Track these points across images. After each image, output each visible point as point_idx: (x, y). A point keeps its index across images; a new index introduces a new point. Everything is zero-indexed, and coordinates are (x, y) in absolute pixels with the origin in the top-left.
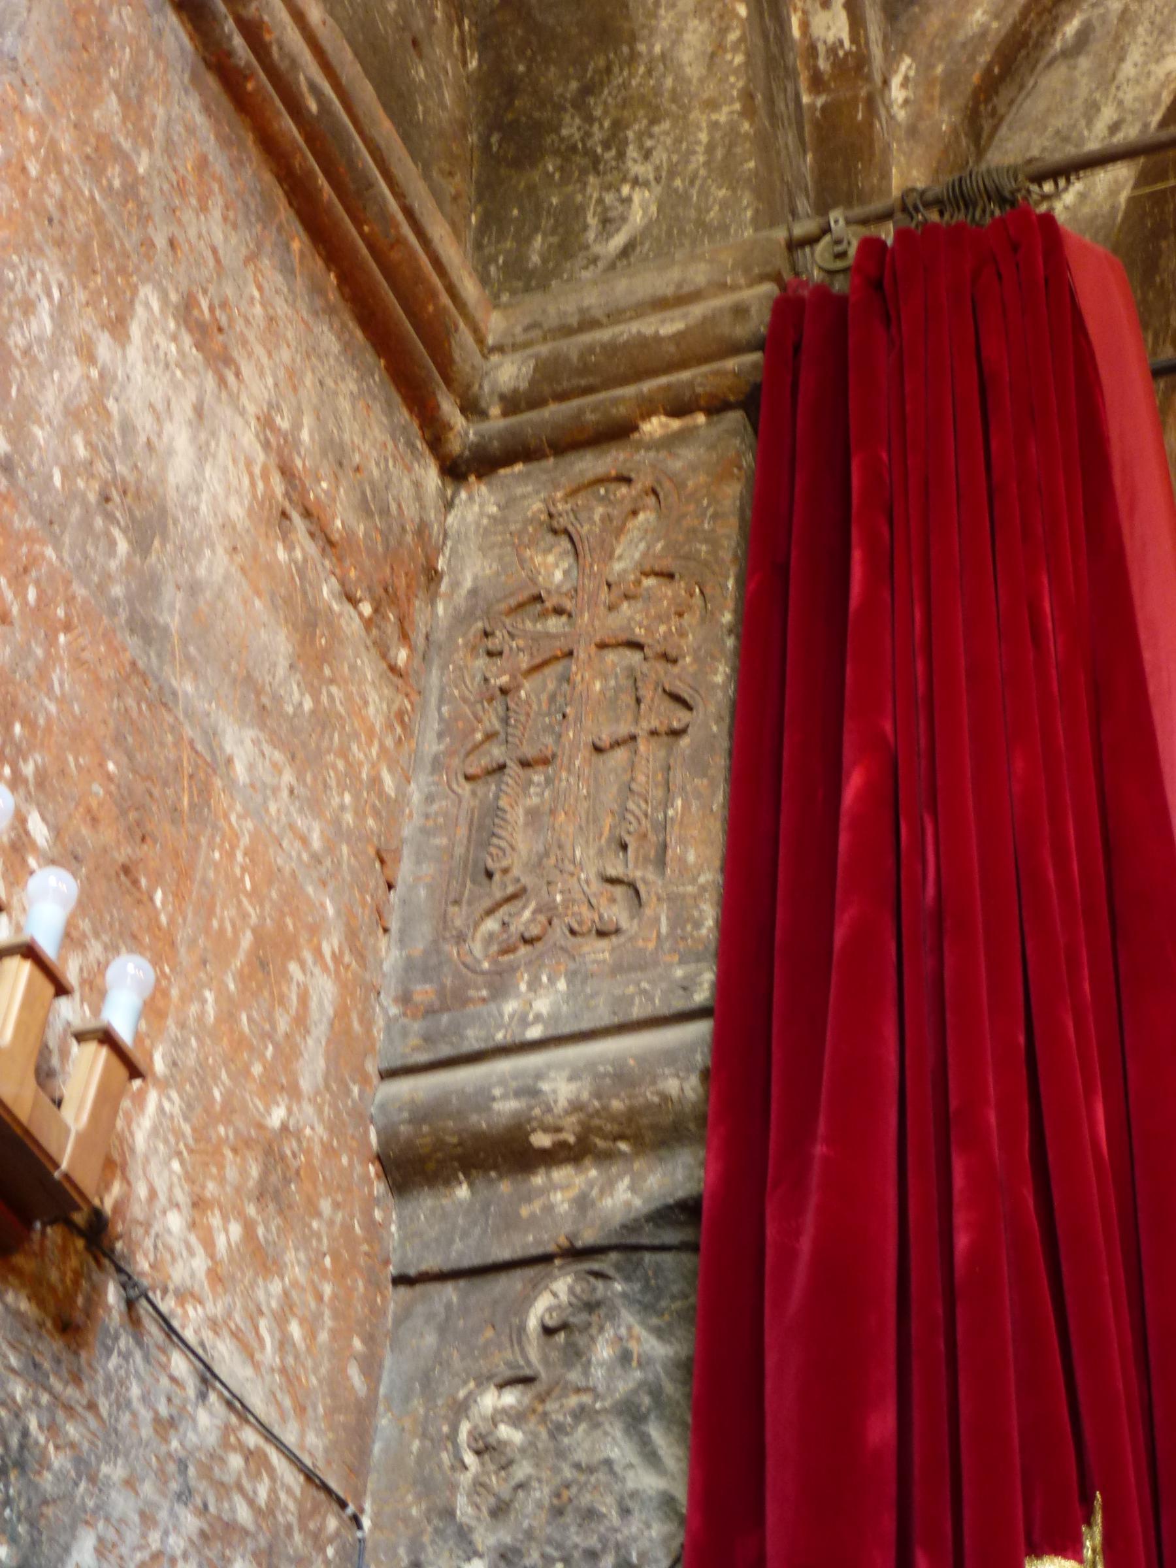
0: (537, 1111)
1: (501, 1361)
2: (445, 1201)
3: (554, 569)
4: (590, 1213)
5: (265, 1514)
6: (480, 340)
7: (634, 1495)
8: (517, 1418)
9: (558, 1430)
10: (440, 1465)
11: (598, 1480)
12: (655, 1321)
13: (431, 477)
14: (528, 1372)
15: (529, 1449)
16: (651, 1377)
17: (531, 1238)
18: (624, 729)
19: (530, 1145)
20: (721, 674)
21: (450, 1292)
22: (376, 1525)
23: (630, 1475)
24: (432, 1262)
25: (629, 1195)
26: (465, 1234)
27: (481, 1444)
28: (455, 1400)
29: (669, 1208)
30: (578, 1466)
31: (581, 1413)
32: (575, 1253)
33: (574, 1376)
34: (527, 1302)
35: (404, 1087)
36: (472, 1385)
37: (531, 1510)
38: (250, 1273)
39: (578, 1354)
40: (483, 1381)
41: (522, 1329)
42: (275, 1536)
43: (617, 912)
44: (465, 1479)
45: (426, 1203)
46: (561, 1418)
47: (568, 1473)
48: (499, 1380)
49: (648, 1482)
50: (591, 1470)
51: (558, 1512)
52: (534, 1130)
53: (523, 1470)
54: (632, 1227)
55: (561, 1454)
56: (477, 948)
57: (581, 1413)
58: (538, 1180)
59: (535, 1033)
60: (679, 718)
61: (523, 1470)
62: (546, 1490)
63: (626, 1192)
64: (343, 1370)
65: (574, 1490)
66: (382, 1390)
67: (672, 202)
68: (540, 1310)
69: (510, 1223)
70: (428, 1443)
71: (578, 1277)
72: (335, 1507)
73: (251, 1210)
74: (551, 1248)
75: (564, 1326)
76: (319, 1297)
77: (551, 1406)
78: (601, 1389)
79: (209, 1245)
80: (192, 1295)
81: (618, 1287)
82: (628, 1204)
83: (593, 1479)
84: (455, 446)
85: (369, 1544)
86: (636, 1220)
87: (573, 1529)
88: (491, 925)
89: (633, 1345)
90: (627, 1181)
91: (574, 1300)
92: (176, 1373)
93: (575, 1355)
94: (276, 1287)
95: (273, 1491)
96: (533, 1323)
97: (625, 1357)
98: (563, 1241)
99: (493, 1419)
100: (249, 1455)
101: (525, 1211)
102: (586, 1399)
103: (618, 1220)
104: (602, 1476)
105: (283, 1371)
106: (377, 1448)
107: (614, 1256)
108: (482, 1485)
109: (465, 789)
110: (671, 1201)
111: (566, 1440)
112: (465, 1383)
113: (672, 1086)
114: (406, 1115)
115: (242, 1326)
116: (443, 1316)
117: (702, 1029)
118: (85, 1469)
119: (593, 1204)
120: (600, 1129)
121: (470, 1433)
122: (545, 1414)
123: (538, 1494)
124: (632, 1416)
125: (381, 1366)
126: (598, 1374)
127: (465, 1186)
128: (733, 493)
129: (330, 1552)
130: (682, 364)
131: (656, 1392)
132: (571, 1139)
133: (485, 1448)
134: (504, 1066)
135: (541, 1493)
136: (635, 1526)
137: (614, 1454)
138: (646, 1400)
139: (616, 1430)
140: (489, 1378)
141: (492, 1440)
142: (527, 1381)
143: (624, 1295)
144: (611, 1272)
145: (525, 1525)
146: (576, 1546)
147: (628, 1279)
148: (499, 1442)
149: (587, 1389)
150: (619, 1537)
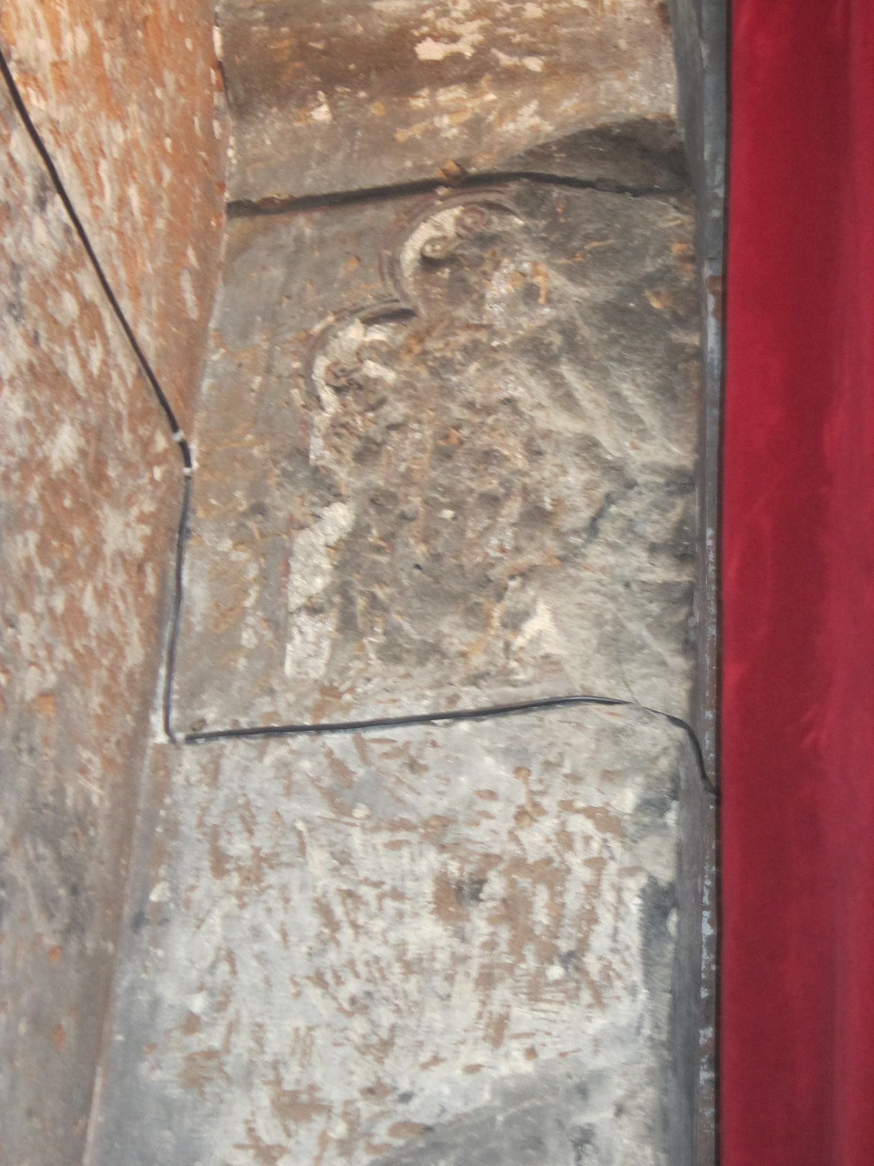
0: (429, 14)
1: (370, 292)
2: (297, 125)
4: (486, 139)
7: (546, 435)
8: (388, 355)
10: (289, 403)
11: (497, 420)
12: (563, 261)
14: (403, 305)
15: (406, 388)
16: (563, 316)
17: (409, 164)
19: (415, 55)
21: (304, 225)
22: (203, 466)
23: (538, 414)
24: (279, 191)
25: (536, 120)
26: (324, 159)
27: (343, 381)
28: (309, 336)
29: (590, 134)
30: (470, 405)
31: (472, 351)
32: (464, 182)
33: (463, 312)
34: (402, 233)
36: (331, 319)
37: (411, 450)
38: (93, 100)
39: (468, 290)
40: (344, 315)
41: (394, 263)
42: (105, 419)
44: (321, 419)
46: (449, 354)
47: (457, 412)
48: (363, 314)
50: (488, 410)
51: (445, 455)
52: (422, 38)
53: (397, 410)
54: (540, 152)
55: (448, 392)
58: (419, 103)
61: (397, 410)
62: (428, 432)
64: (177, 276)
65: (465, 432)
66: (212, 325)
68: (420, 239)
69: (383, 143)
70: (273, 379)
71: (469, 208)
72: (165, 423)
73: (99, 27)
74: (437, 174)
75: (451, 260)
76: (159, 177)
77: (434, 345)
78: (499, 325)
79: (57, 37)
80: (35, 79)
81: (519, 222)
82: (535, 129)
83: (490, 420)
85: (196, 486)
86: (545, 146)
87: (465, 473)
89: (539, 280)
90: (534, 105)
91: (463, 232)
92: (17, 157)
93: (463, 291)
94: (119, 135)
95: (105, 363)
96: (409, 255)
97: (530, 294)
98: (451, 166)
99: (358, 354)
100: (86, 306)
101: (402, 135)
102: (482, 336)
103: (523, 145)
104: (503, 416)
105: (121, 234)
106: (206, 384)
107: (514, 187)
108: (344, 426)
110: (591, 127)
111: (455, 379)
112: (322, 316)
114: (260, 14)
115: (83, 152)
116: (292, 249)
119: (490, 128)
120: (506, 38)
121: (328, 369)
122: (425, 352)
123: (418, 436)
125: (212, 298)
126: (495, 312)
127: (325, 109)
129: (158, 473)
131: (569, 332)
132: (468, 53)
133: (347, 384)
135: (422, 433)
136: (547, 469)
137: (519, 392)
138: (556, 340)
139: (522, 368)
140: (354, 312)
141: (356, 376)
142: (402, 315)
143: (526, 230)
144: (510, 205)
145: (403, 467)
146: (471, 491)
147: (530, 214)
148: (367, 378)
149: (480, 327)
150: (527, 480)
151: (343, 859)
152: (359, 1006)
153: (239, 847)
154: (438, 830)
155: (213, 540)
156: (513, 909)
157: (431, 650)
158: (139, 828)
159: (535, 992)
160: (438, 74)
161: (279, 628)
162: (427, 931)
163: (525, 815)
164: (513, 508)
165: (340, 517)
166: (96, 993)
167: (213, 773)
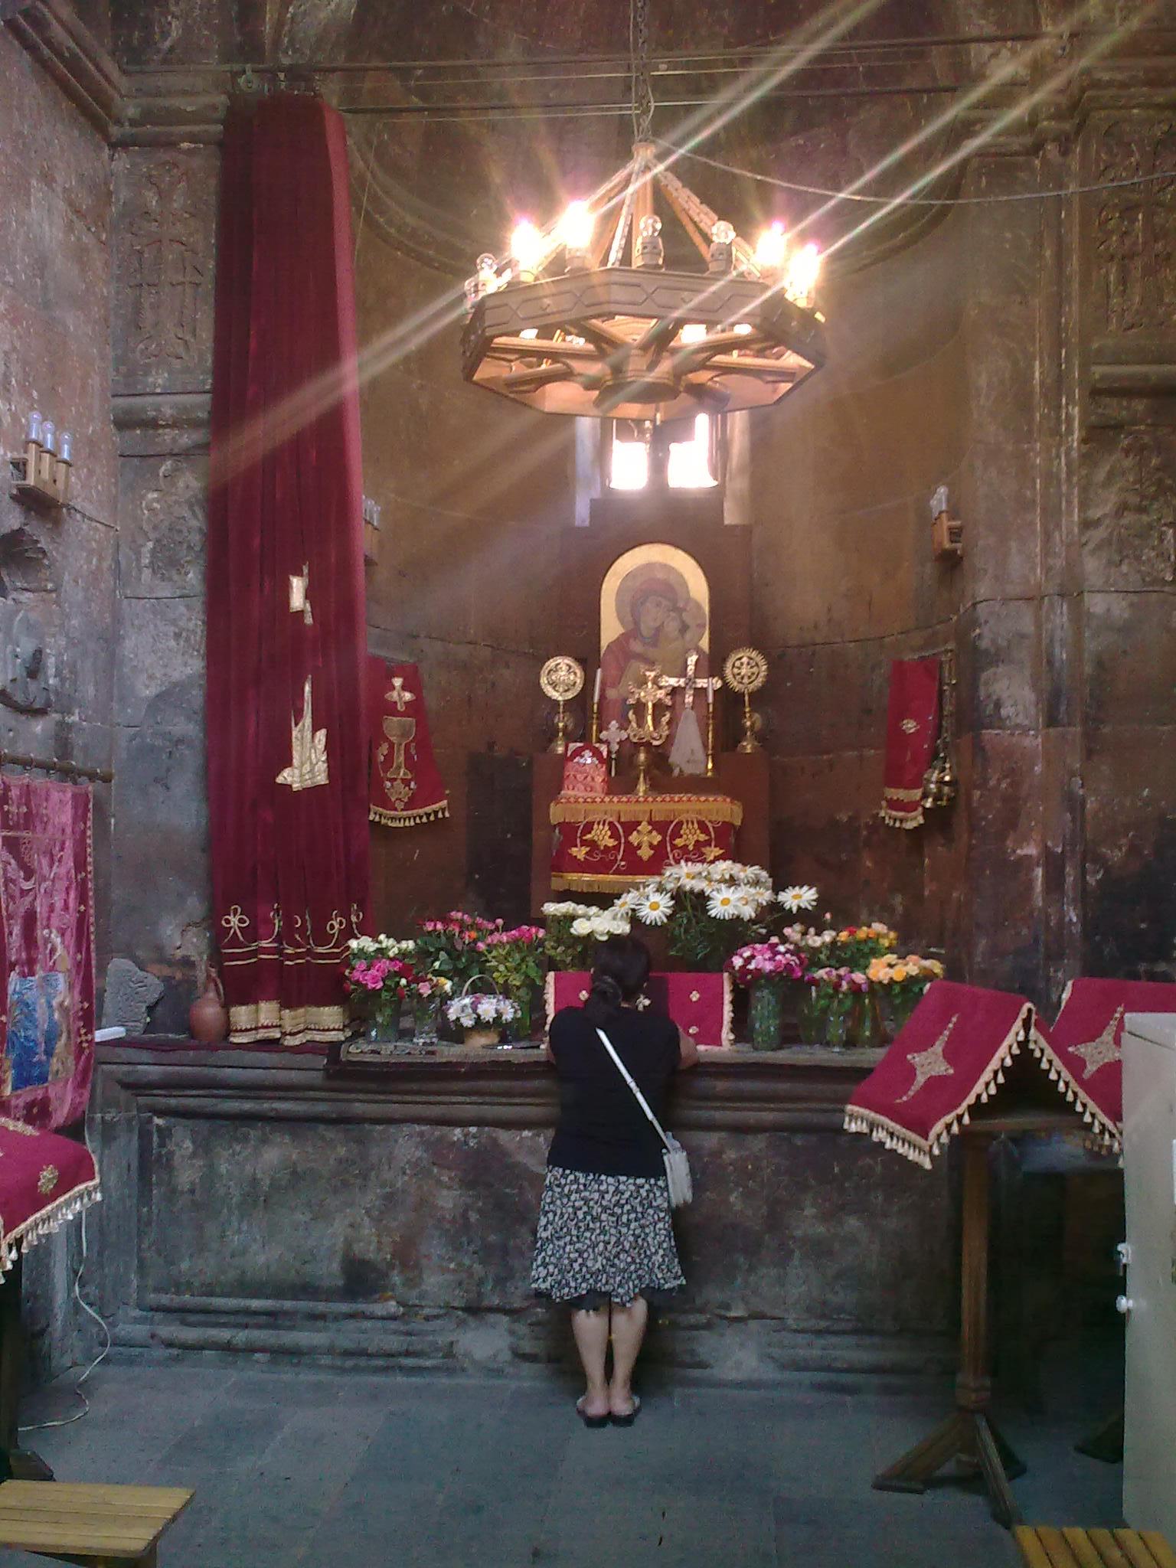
3: (152, 200)
5: (98, 542)
6: (119, 92)
8: (158, 501)
9: (170, 506)
13: (106, 152)
18: (181, 279)
20: (211, 265)
21: (136, 461)
35: (120, 401)
40: (149, 489)
43: (181, 351)
45: (127, 434)
49: (195, 523)
53: (161, 517)
54: (188, 449)
56: (138, 354)
57: (176, 502)
59: (158, 390)
60: (198, 279)
63: (186, 439)
67: (187, 29)
84: (113, 140)
88: (141, 346)
93: (174, 485)
109: (128, 290)
113: (200, 415)
117: (208, 396)
118: (64, 556)
124: (191, 506)
128: (213, 182)
130: (196, 122)
134: (150, 399)
135: (166, 523)
151: (156, 626)
152: (161, 658)
153: (136, 622)
154: (174, 622)
155: (125, 549)
156: (187, 640)
157: (170, 579)
158: (118, 619)
159: (192, 656)
160: (162, 426)
161: (140, 571)
162: (172, 643)
163: (190, 619)
164: (185, 546)
165: (150, 545)
166: (113, 654)
167: (130, 605)
